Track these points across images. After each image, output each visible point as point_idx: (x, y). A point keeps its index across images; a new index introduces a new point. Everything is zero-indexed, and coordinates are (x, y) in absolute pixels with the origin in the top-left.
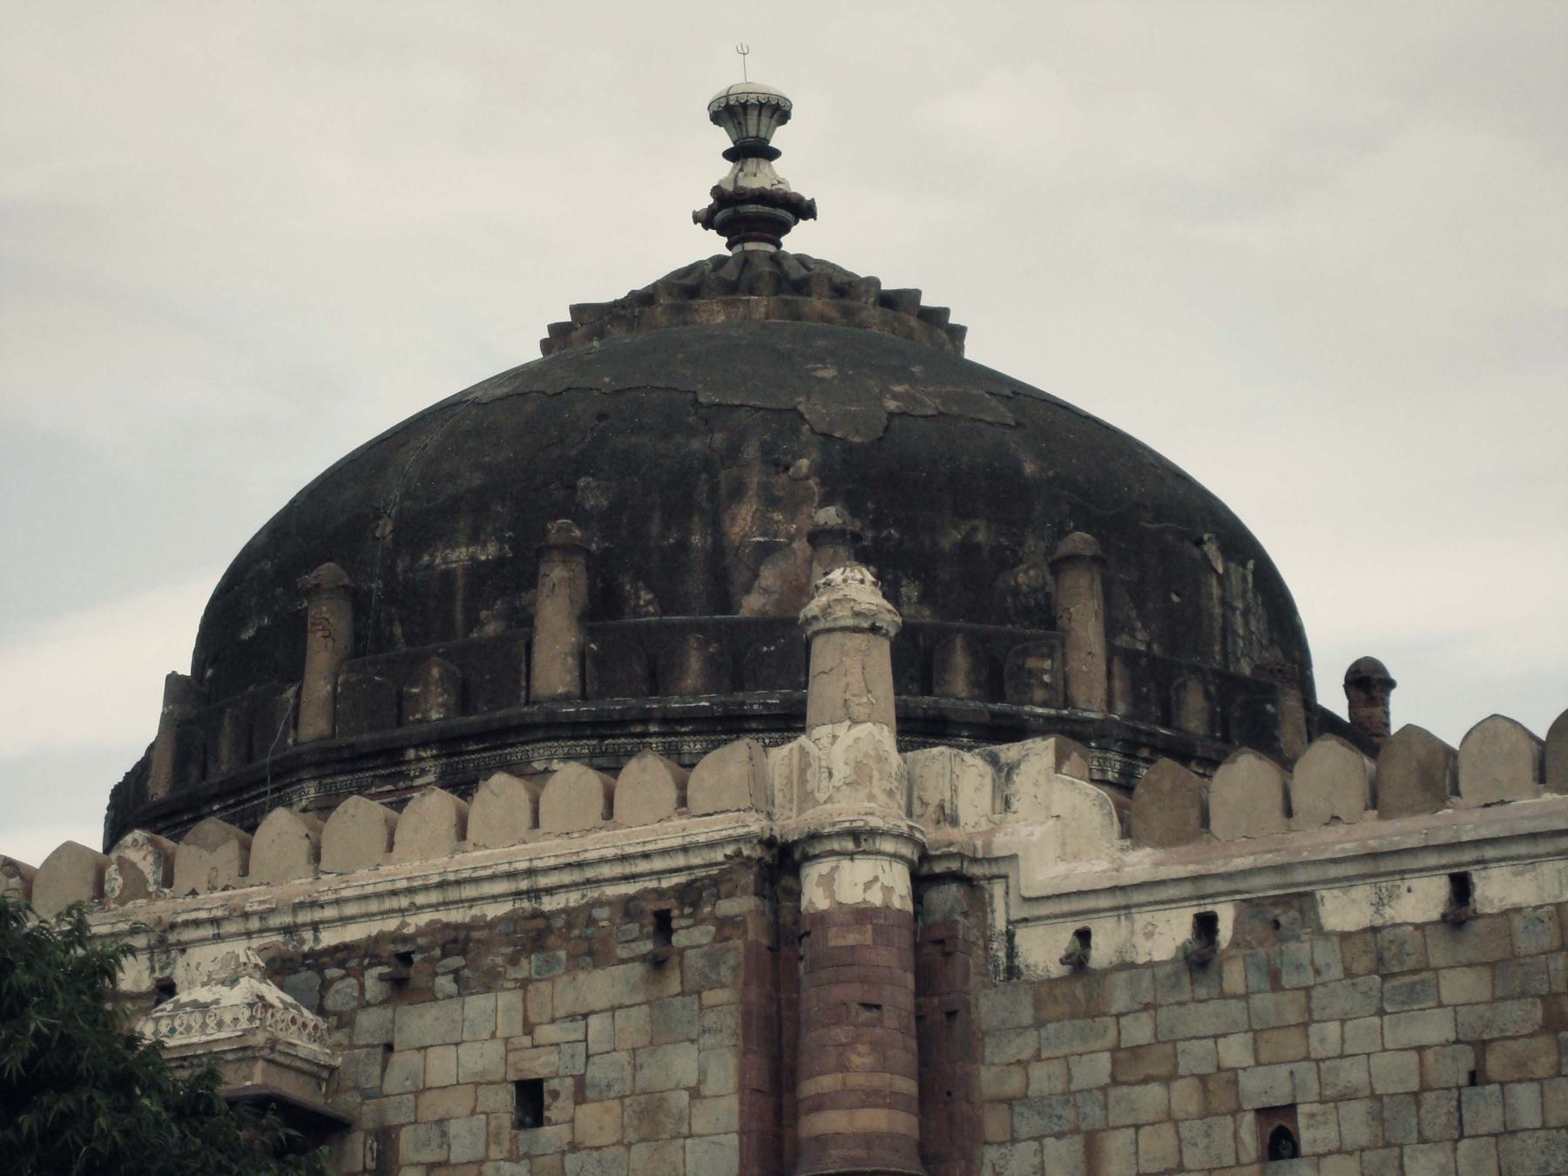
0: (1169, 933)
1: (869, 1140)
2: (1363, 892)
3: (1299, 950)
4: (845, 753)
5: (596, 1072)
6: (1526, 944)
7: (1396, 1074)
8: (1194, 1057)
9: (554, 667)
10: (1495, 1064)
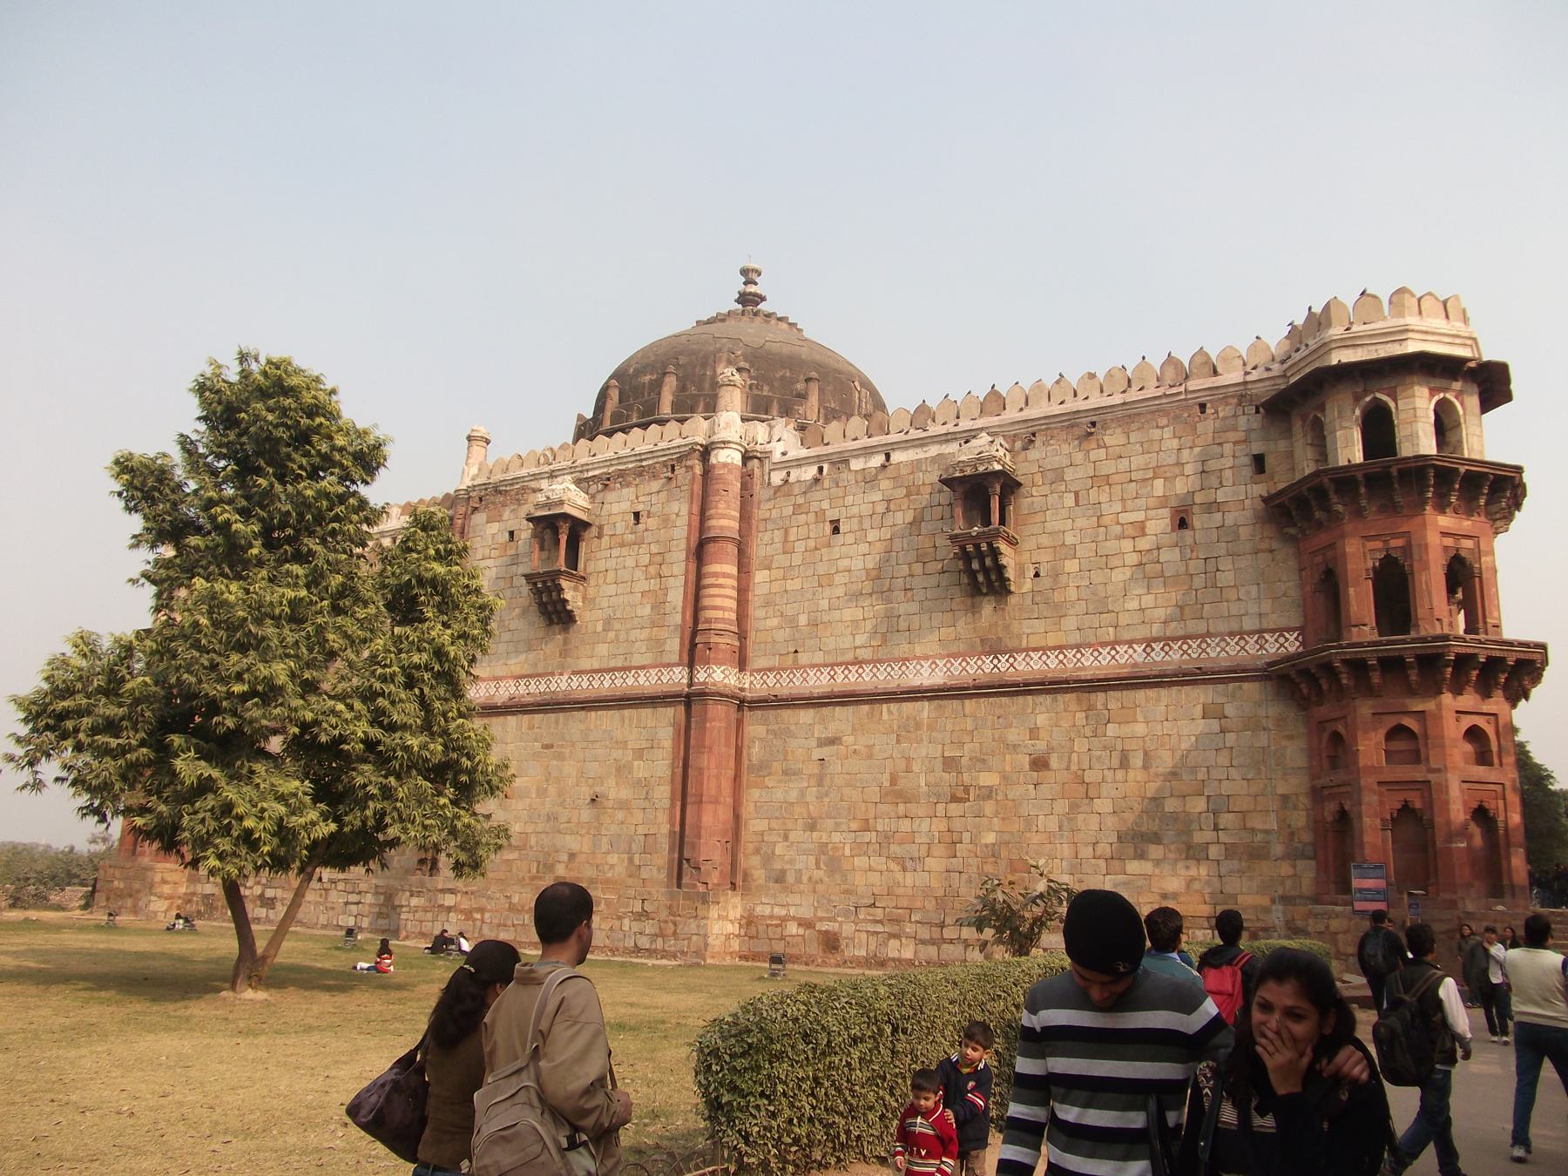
0: (812, 471)
1: (722, 528)
2: (862, 460)
3: (844, 476)
4: (730, 423)
5: (653, 509)
6: (903, 472)
7: (866, 509)
8: (814, 506)
9: (666, 409)
10: (892, 507)
